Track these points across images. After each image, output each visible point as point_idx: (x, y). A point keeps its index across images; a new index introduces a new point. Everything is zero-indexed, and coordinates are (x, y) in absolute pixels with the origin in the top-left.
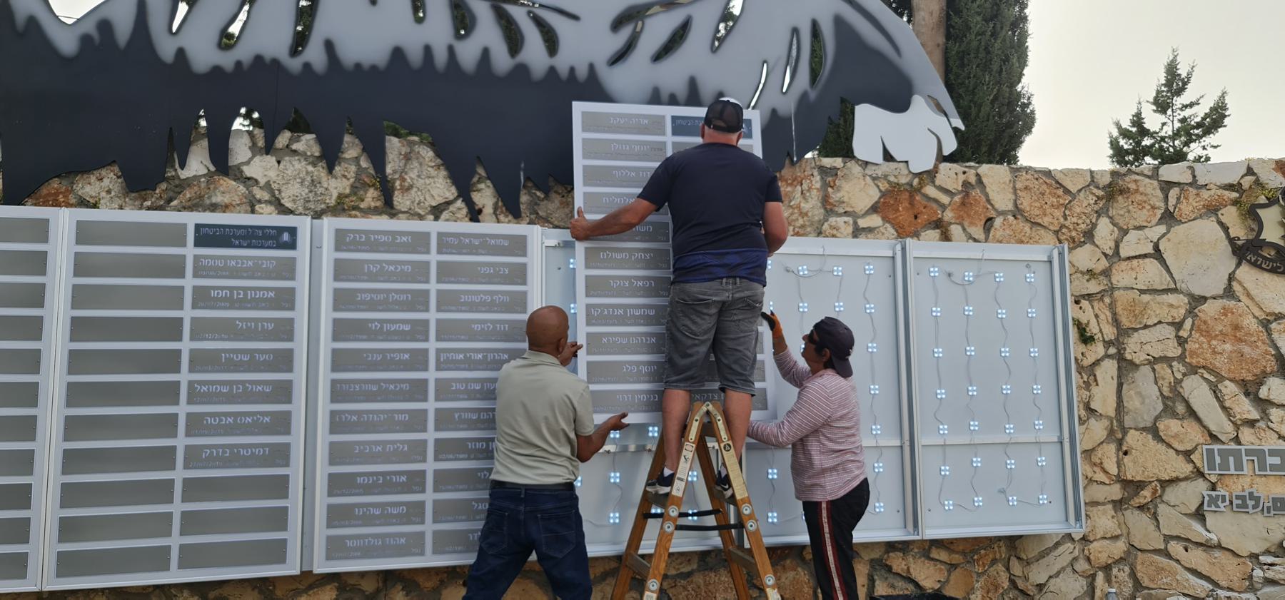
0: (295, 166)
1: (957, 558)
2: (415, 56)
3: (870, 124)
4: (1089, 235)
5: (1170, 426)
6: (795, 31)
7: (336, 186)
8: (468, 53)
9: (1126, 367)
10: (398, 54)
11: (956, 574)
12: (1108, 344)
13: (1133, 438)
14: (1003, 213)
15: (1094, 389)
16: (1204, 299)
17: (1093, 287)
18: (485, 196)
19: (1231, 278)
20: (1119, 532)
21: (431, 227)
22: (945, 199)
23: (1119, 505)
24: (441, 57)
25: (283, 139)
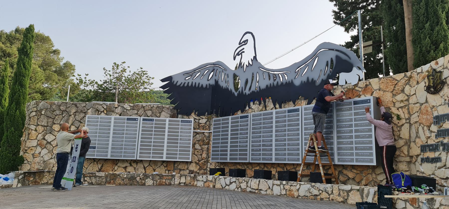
0: (257, 105)
1: (359, 172)
2: (269, 86)
3: (343, 77)
4: (403, 91)
5: (417, 140)
6: (327, 62)
7: (261, 108)
8: (275, 83)
9: (411, 125)
10: (267, 86)
11: (358, 175)
12: (406, 119)
13: (412, 144)
14: (376, 90)
15: (401, 132)
16: (422, 104)
17: (402, 105)
18: (277, 106)
19: (427, 98)
20: (408, 170)
21: (262, 112)
22: (360, 90)
23: (409, 163)
24: (272, 84)
25: (255, 102)
